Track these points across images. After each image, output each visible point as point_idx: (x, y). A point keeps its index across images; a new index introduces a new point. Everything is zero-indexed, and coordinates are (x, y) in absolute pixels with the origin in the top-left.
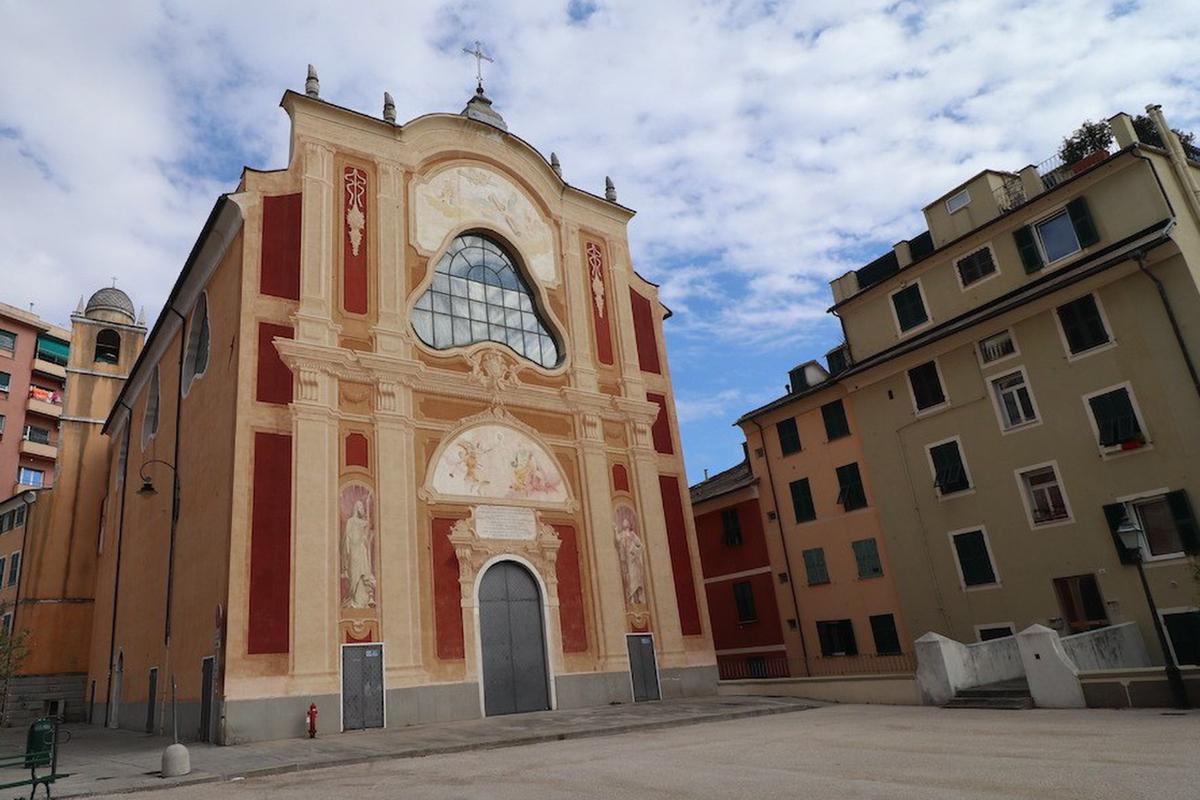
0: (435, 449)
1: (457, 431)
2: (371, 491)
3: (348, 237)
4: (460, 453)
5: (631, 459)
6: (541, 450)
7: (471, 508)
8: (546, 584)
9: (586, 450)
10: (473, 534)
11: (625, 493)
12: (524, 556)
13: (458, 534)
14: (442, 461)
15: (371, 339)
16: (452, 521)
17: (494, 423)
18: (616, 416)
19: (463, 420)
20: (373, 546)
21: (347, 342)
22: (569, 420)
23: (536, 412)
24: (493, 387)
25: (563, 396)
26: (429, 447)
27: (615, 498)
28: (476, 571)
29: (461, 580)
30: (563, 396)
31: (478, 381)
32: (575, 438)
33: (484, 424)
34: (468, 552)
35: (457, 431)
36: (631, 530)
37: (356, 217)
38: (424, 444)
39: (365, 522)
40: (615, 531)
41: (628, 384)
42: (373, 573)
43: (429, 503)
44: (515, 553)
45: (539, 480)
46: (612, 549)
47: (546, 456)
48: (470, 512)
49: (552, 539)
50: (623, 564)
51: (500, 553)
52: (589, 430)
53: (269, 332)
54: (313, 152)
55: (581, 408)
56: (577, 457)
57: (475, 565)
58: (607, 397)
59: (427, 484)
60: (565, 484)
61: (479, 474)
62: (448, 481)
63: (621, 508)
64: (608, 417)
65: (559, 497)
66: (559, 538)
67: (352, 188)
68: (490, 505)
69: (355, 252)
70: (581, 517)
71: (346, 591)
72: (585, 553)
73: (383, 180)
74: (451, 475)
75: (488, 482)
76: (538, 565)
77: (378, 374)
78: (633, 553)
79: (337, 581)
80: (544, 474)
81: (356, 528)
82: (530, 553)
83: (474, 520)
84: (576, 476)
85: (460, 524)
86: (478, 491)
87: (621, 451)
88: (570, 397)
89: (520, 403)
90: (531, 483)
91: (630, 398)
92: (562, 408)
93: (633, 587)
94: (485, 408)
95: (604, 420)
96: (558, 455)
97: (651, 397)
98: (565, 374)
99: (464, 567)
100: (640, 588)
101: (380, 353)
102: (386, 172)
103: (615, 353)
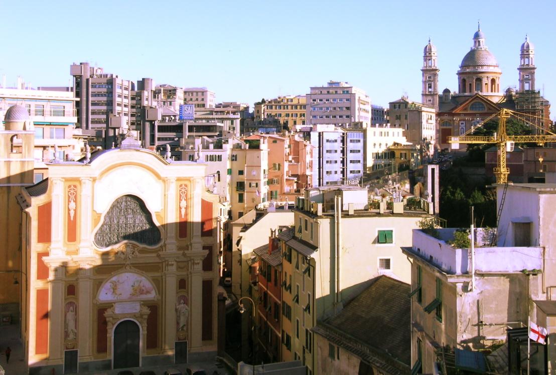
0: (100, 285)
2: (76, 303)
3: (69, 214)
4: (110, 286)
5: (190, 276)
7: (113, 304)
8: (142, 327)
9: (167, 276)
10: (113, 313)
11: (185, 290)
12: (133, 318)
13: (108, 313)
14: (103, 289)
15: (77, 250)
16: (106, 309)
17: (126, 272)
18: (185, 259)
19: (113, 273)
20: (76, 319)
21: (68, 253)
22: (160, 265)
24: (126, 259)
25: (159, 256)
26: (98, 285)
27: (179, 292)
28: (113, 325)
29: (108, 328)
30: (159, 256)
31: (120, 257)
32: (162, 271)
33: (121, 273)
34: (111, 319)
36: (184, 303)
37: (72, 205)
39: (74, 313)
40: (176, 305)
41: (193, 245)
42: (76, 328)
44: (130, 317)
45: (143, 290)
46: (174, 312)
47: (147, 281)
48: (113, 306)
49: (147, 311)
50: (178, 317)
51: (124, 318)
52: (170, 268)
53: (40, 255)
54: (56, 183)
55: (167, 259)
56: (162, 279)
57: (114, 323)
58: (181, 252)
59: (97, 298)
60: (155, 291)
61: (118, 292)
62: (105, 295)
63: (181, 296)
64: (180, 260)
65: (152, 296)
66: (150, 310)
67: (71, 194)
69: (72, 219)
71: (67, 335)
72: (160, 314)
73: (83, 185)
75: (121, 294)
76: (139, 320)
77: (79, 262)
78: (183, 312)
79: (63, 331)
81: (70, 316)
82: (136, 317)
84: (161, 286)
85: (108, 310)
87: (185, 273)
88: (162, 256)
89: (137, 262)
91: (193, 250)
92: (158, 260)
93: (181, 325)
94: (122, 267)
95: (178, 262)
96: (153, 280)
97: (204, 248)
98: (161, 247)
99: (109, 324)
100: (185, 325)
101: (81, 255)
102: (84, 183)
103: (188, 232)
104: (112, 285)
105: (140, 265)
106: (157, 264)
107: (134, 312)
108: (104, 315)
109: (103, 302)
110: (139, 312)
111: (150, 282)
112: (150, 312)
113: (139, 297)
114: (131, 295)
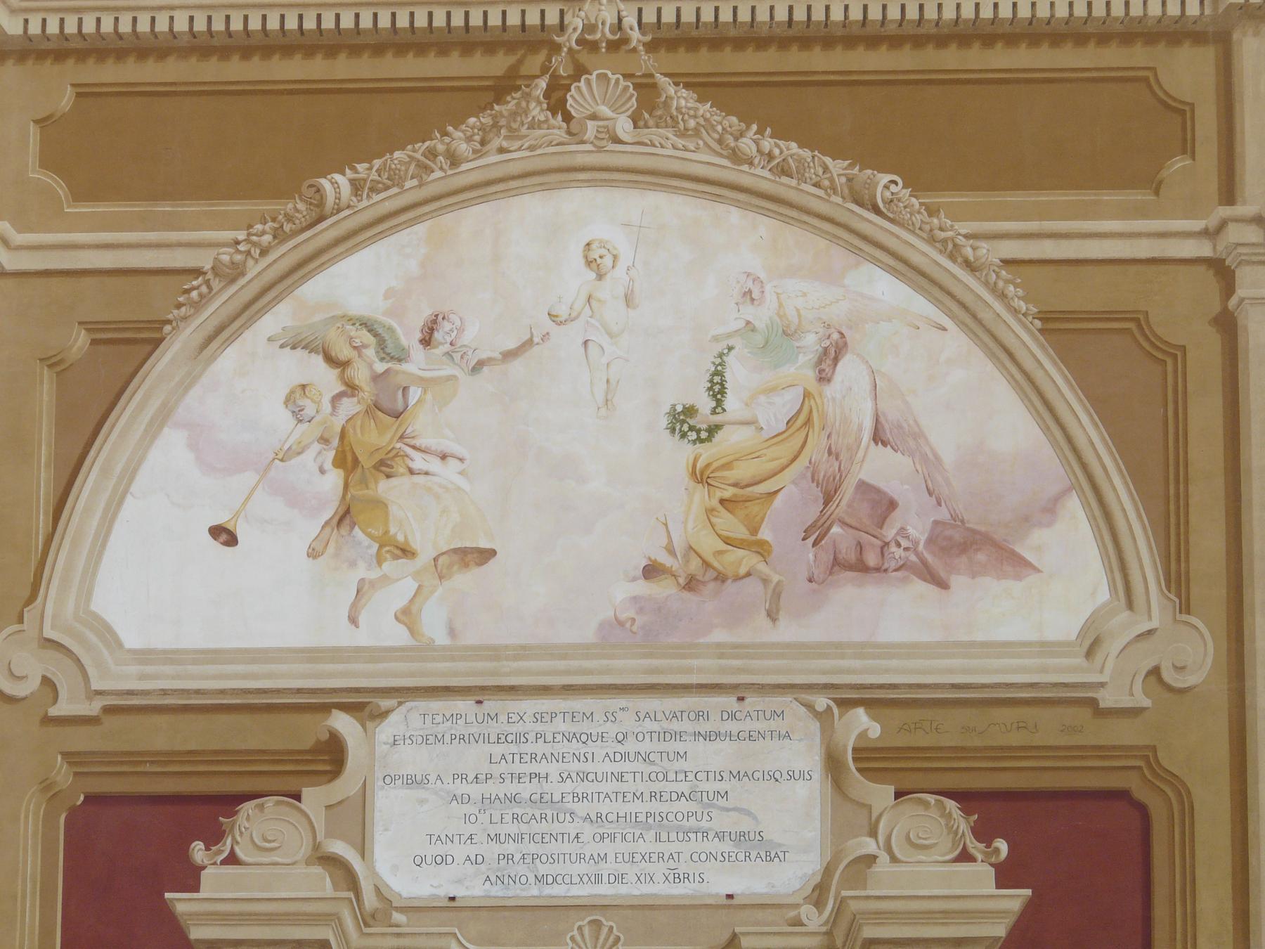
1: (286, 257)
4: (296, 397)
6: (920, 305)
7: (343, 723)
19: (336, 185)
23: (904, 60)
33: (485, 189)
35: (286, 257)
38: (53, 362)
43: (62, 708)
47: (956, 342)
66: (1006, 876)
68: (479, 693)
70: (1220, 727)
74: (224, 535)
80: (929, 462)
83: (363, 799)
86: (407, 616)
90: (816, 532)
94: (502, 88)
104: (326, 379)
105: (819, 61)
106: (1112, 57)
107: (720, 882)
108: (181, 902)
109: (167, 679)
110: (818, 895)
111: (1003, 354)
112: (1015, 899)
113: (787, 631)
114: (651, 571)
